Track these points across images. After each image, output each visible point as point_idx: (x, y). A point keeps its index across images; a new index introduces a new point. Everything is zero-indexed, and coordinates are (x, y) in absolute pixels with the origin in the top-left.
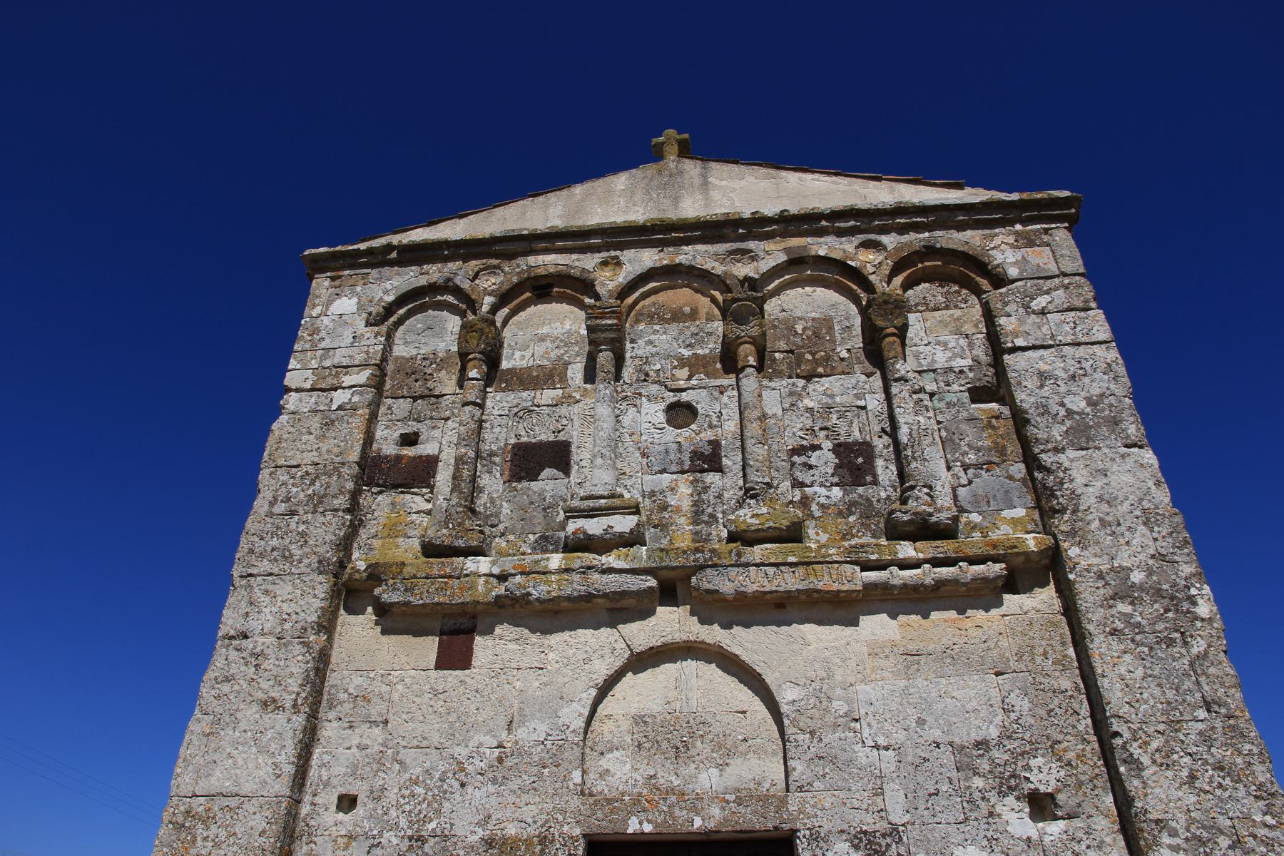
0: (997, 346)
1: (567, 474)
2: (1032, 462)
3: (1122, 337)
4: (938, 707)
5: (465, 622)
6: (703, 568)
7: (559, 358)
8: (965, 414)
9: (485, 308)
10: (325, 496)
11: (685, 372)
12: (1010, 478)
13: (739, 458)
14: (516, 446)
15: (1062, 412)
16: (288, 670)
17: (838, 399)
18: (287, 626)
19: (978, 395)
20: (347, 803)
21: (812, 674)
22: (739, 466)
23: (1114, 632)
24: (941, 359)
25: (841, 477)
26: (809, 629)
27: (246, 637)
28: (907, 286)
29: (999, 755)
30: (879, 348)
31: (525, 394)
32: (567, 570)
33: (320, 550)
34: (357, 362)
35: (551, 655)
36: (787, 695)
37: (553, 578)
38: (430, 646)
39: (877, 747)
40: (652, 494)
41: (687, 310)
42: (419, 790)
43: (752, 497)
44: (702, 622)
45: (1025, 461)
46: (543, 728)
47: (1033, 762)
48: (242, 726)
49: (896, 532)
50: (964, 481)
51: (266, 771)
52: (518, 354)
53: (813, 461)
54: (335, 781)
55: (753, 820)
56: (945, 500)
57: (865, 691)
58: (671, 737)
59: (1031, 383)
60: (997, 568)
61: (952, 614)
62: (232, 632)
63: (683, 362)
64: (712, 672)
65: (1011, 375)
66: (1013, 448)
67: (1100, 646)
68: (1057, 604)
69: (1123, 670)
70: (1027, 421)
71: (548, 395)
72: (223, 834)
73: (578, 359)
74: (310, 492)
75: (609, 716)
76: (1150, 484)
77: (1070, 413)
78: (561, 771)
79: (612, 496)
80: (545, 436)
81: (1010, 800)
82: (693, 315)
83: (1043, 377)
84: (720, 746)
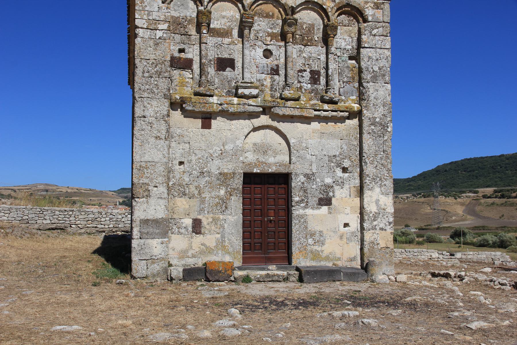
0: (359, 45)
1: (234, 70)
2: (360, 84)
3: (393, 49)
4: (326, 146)
5: (209, 116)
6: (275, 107)
7: (230, 26)
8: (346, 65)
9: (206, 4)
10: (161, 72)
11: (269, 39)
12: (354, 87)
13: (284, 72)
14: (219, 59)
15: (372, 71)
16: (161, 128)
17: (313, 55)
18: (158, 115)
19: (351, 58)
20: (181, 163)
21: (298, 136)
22: (284, 74)
23: (369, 133)
24: (343, 45)
25: (311, 81)
26: (299, 124)
27: (145, 117)
28: (339, 15)
29: (338, 159)
30: (326, 40)
31: (219, 39)
32: (239, 104)
33: (164, 91)
34: (162, 19)
35: (233, 126)
36: (292, 141)
37: (235, 106)
38: (199, 122)
39: (312, 155)
40: (259, 80)
41: (271, 13)
42: (200, 161)
43: (288, 86)
44: (272, 120)
45: (359, 83)
46: (232, 146)
47: (345, 161)
48: (151, 143)
49: (323, 101)
50: (342, 87)
51: (161, 156)
52: (216, 22)
53: (304, 75)
54: (177, 158)
55: (283, 170)
56: (337, 92)
57: (310, 141)
58: (262, 149)
59: (366, 59)
60: (346, 114)
61: (333, 124)
62: (140, 116)
63: (269, 35)
64: (273, 133)
65: (361, 56)
66: (357, 78)
67: (365, 136)
68: (358, 123)
69: (369, 142)
70: (362, 72)
71: (227, 40)
72: (152, 172)
73: (236, 28)
74: (156, 70)
75: (247, 143)
76: (387, 95)
77: (374, 71)
78: (237, 157)
79: (251, 83)
80: (226, 56)
81: (339, 169)
82: (272, 16)
83: (370, 58)
84: (274, 152)
